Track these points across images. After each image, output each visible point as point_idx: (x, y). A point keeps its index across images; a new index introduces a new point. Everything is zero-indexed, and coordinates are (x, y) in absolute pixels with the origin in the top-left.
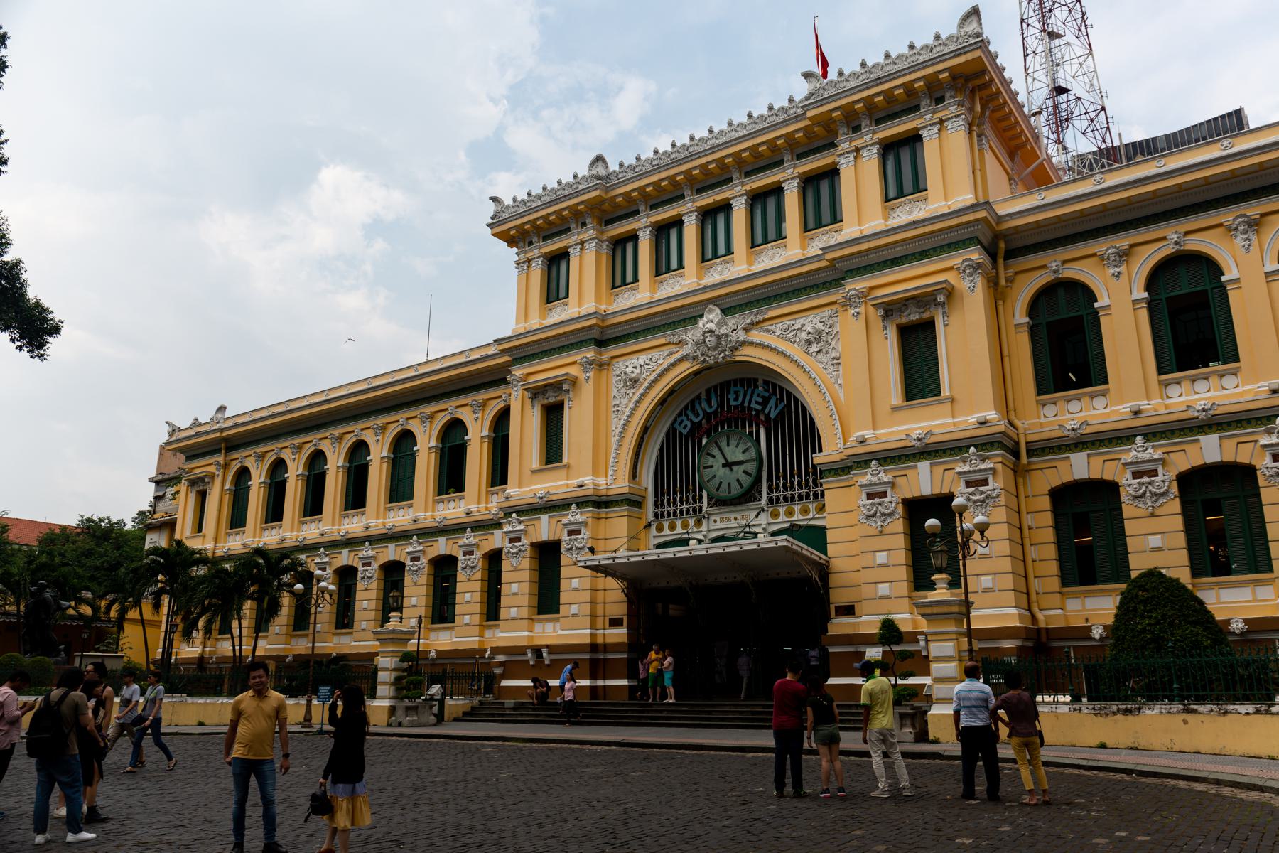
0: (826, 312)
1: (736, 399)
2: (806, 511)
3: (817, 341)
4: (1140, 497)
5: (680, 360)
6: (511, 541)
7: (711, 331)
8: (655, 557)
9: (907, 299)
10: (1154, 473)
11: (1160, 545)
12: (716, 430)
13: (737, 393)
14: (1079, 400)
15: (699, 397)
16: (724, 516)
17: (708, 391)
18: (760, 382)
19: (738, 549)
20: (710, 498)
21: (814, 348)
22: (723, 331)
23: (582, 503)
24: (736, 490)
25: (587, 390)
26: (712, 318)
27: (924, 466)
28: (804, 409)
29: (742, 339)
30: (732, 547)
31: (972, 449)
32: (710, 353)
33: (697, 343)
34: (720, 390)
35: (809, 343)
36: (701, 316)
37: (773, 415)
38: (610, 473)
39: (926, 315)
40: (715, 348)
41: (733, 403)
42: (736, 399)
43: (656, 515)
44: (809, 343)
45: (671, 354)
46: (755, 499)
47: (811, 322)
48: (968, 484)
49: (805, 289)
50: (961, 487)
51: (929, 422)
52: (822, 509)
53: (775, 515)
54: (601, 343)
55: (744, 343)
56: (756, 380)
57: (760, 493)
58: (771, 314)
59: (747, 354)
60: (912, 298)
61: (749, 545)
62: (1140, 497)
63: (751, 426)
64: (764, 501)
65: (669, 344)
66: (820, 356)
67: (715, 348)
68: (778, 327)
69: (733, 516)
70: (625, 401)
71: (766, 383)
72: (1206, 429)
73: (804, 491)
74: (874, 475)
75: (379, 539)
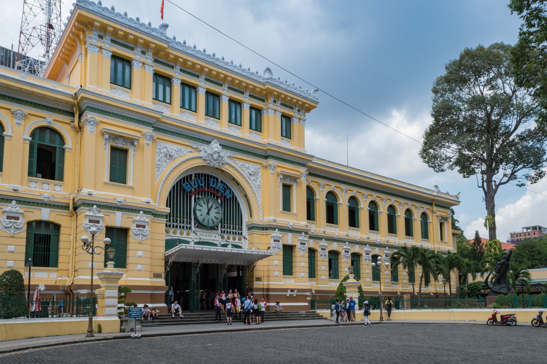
0: (258, 166)
1: (213, 184)
2: (234, 239)
3: (254, 175)
4: (9, 228)
5: (197, 158)
6: (301, 244)
7: (219, 153)
8: (192, 248)
9: (289, 176)
10: (18, 218)
11: (13, 250)
12: (199, 194)
13: (214, 182)
14: (36, 182)
15: (191, 175)
16: (201, 233)
17: (195, 174)
18: (220, 181)
19: (216, 250)
20: (195, 224)
21: (252, 178)
22: (221, 154)
23: (146, 212)
24: (211, 224)
25: (148, 150)
26: (215, 146)
27: (290, 234)
28: (236, 198)
29: (228, 162)
30: (206, 248)
31: (303, 233)
32: (213, 161)
33: (208, 154)
34: (207, 177)
35: (251, 175)
36: (210, 142)
37: (228, 197)
38: (158, 199)
39: (291, 184)
40: (215, 160)
41: (211, 185)
42: (213, 184)
43: (166, 225)
44: (251, 175)
45: (191, 152)
46: (215, 229)
47: (252, 168)
48: (301, 244)
49: (251, 153)
50: (299, 244)
51: (285, 220)
52: (240, 239)
53: (223, 237)
54: (156, 129)
55: (227, 163)
56: (217, 179)
57: (217, 227)
58: (238, 156)
59: (226, 168)
60: (290, 176)
61: (213, 249)
62: (9, 228)
63: (214, 197)
64: (220, 231)
65: (191, 147)
66: (254, 182)
67: (215, 160)
68: (240, 163)
69: (205, 234)
70: (165, 164)
71: (222, 182)
72: (44, 205)
73: (175, 224)
74: (276, 233)
75: (353, 242)
